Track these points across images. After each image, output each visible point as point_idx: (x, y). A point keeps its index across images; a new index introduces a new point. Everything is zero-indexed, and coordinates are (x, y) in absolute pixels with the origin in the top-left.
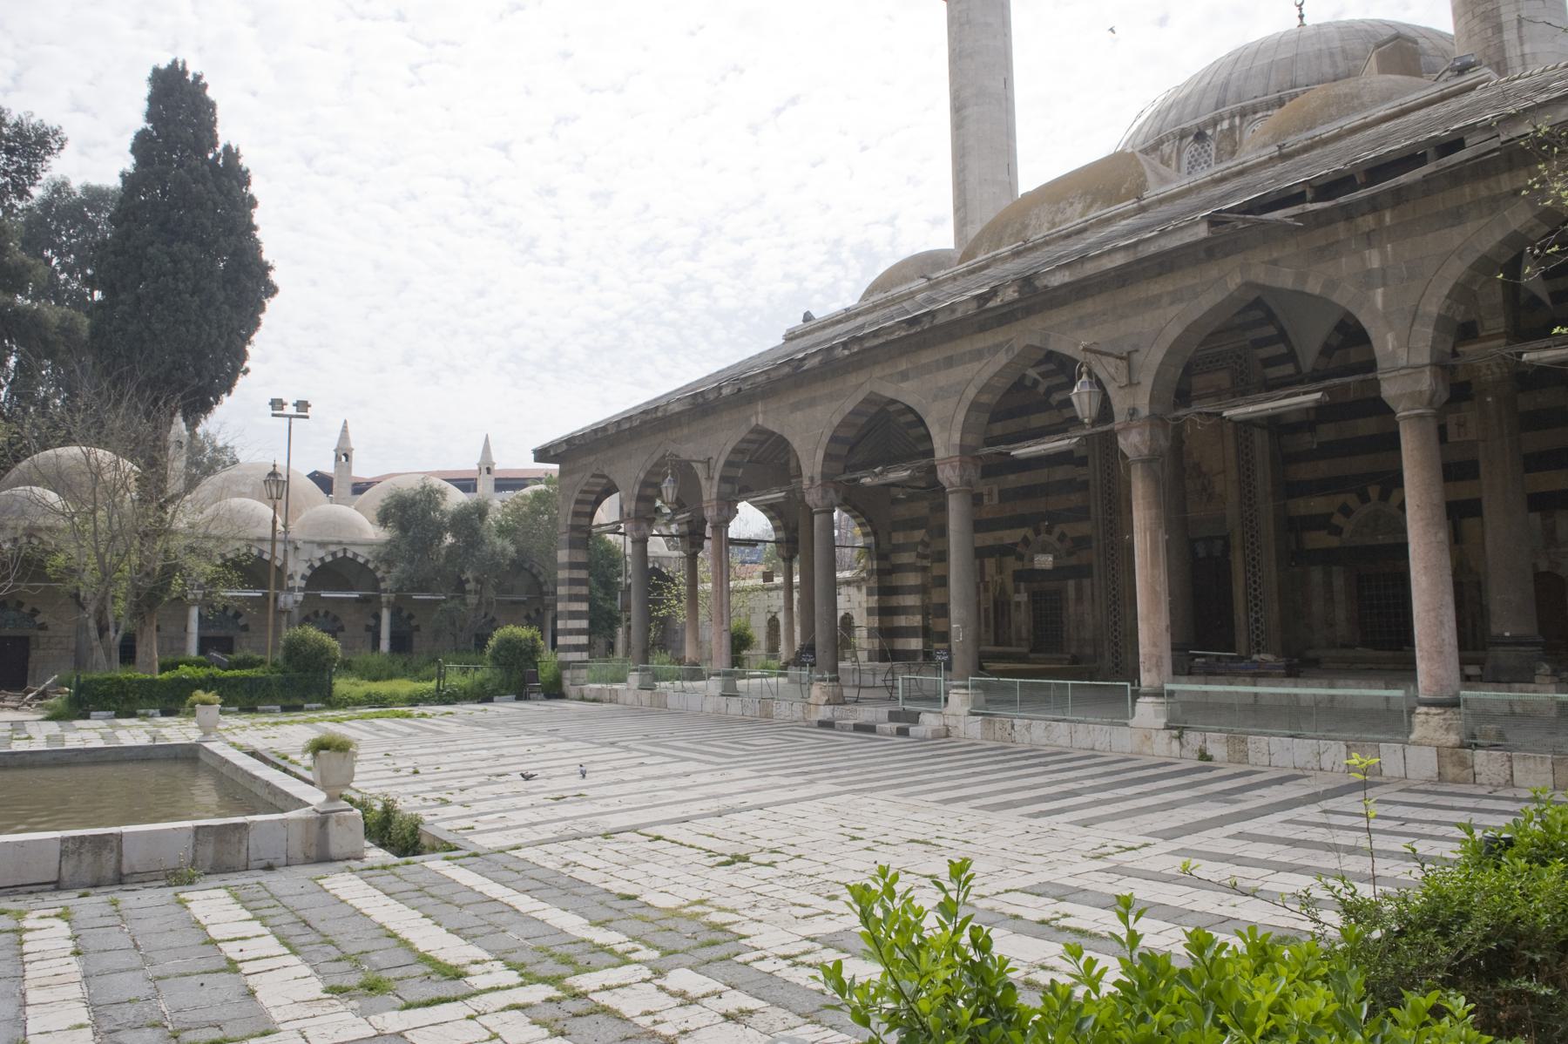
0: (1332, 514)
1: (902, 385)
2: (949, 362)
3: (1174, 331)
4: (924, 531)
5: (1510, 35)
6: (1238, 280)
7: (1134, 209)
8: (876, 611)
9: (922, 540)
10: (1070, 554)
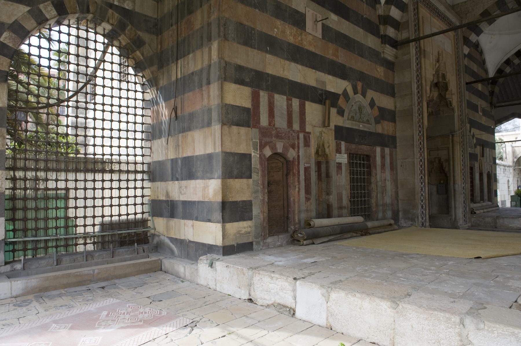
4: (24, 9)
10: (377, 121)
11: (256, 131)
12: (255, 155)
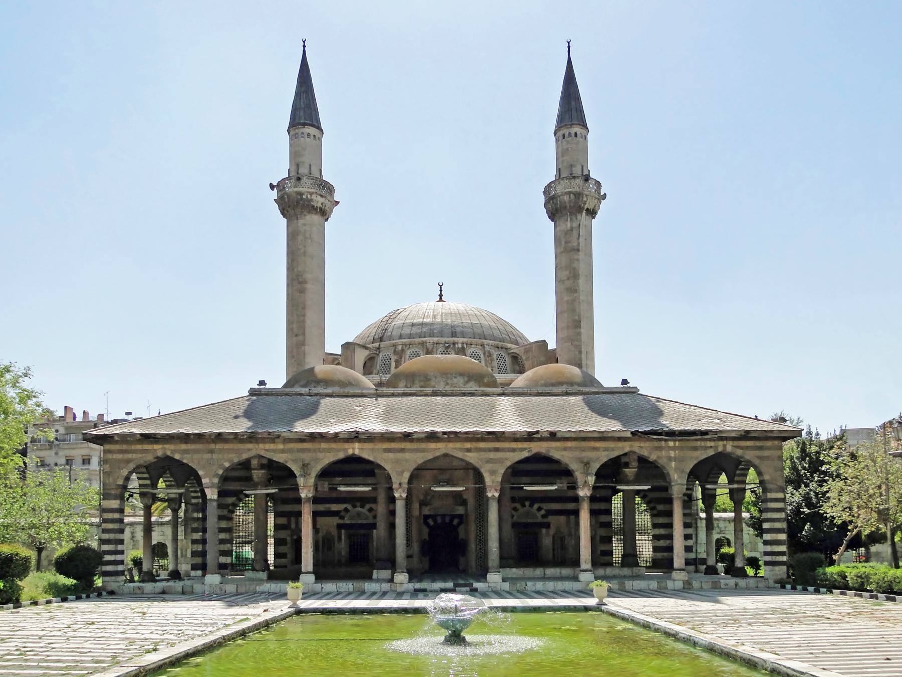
2: (497, 450)
3: (605, 460)
5: (583, 356)
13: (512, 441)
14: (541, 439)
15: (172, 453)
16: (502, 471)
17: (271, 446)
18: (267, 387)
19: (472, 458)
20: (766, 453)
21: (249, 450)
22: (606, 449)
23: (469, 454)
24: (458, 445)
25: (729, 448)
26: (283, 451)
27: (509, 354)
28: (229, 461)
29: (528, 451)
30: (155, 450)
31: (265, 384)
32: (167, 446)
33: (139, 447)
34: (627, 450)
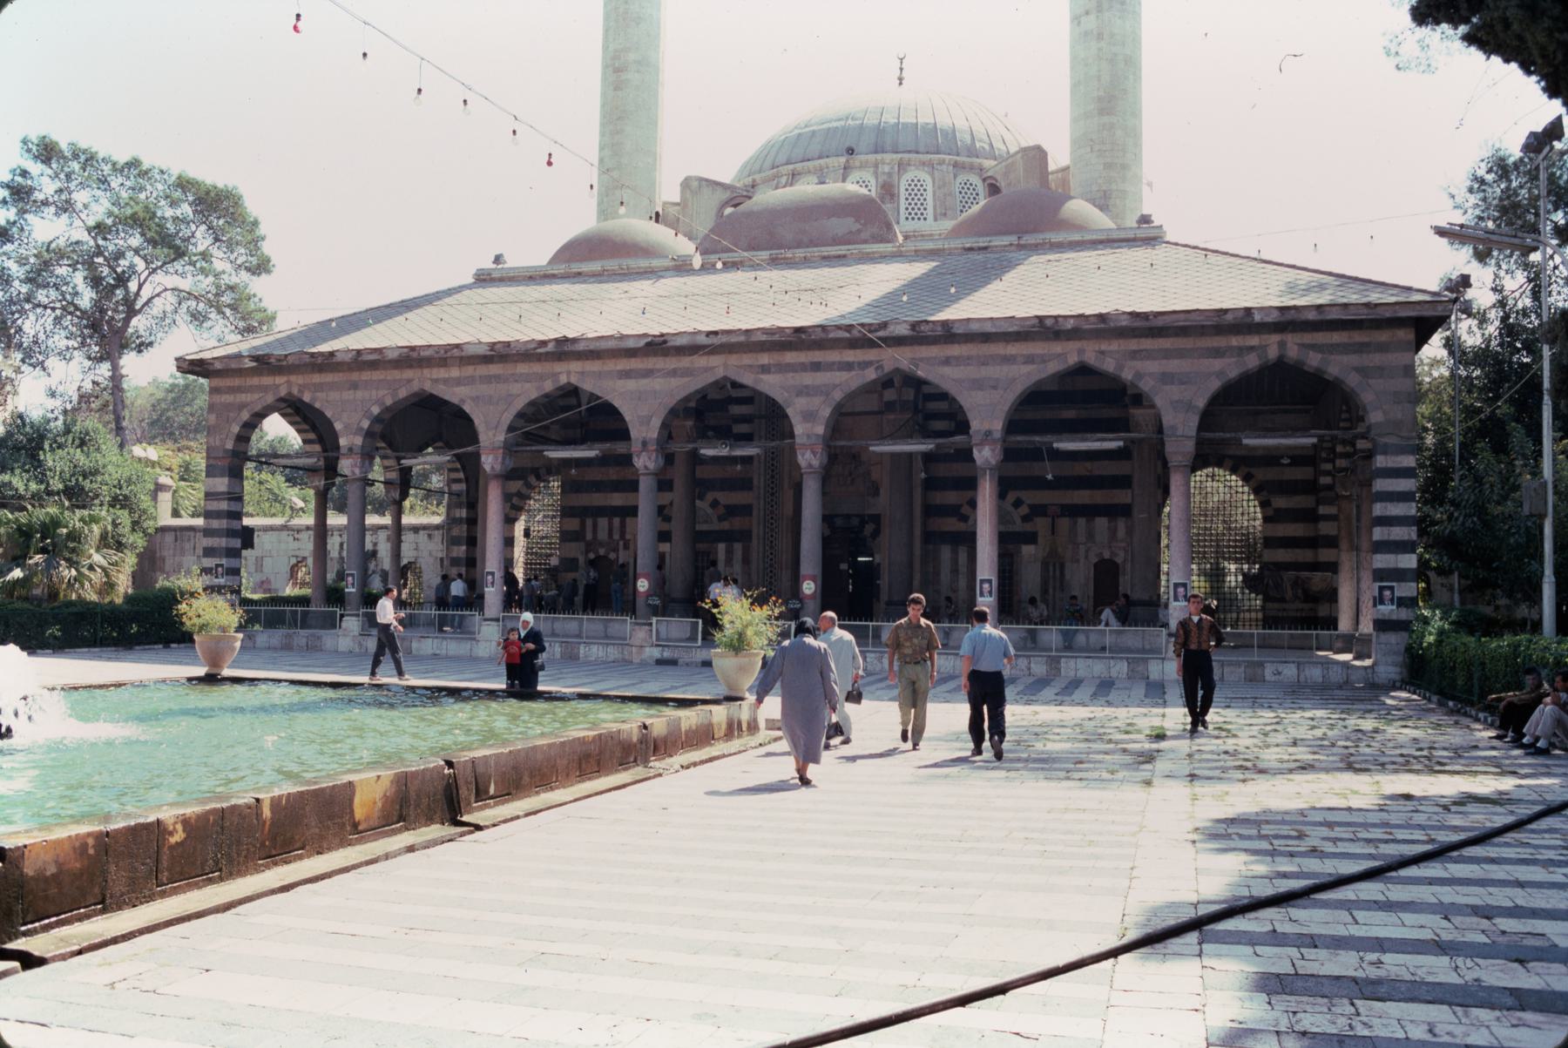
0: (961, 506)
1: (762, 376)
2: (816, 367)
4: (521, 483)
6: (1076, 359)
7: (893, 252)
8: (464, 562)
9: (519, 491)
10: (721, 519)
11: (582, 545)
12: (581, 560)
13: (845, 348)
14: (899, 341)
15: (300, 391)
16: (826, 412)
17: (441, 373)
18: (506, 266)
19: (771, 385)
20: (1376, 359)
21: (409, 381)
22: (1030, 360)
23: (765, 377)
24: (747, 359)
25: (1293, 352)
26: (459, 382)
27: (984, 180)
28: (379, 402)
29: (877, 369)
30: (278, 386)
31: (505, 262)
32: (293, 378)
33: (255, 381)
34: (1073, 360)
